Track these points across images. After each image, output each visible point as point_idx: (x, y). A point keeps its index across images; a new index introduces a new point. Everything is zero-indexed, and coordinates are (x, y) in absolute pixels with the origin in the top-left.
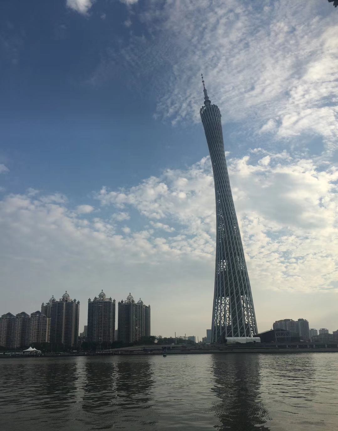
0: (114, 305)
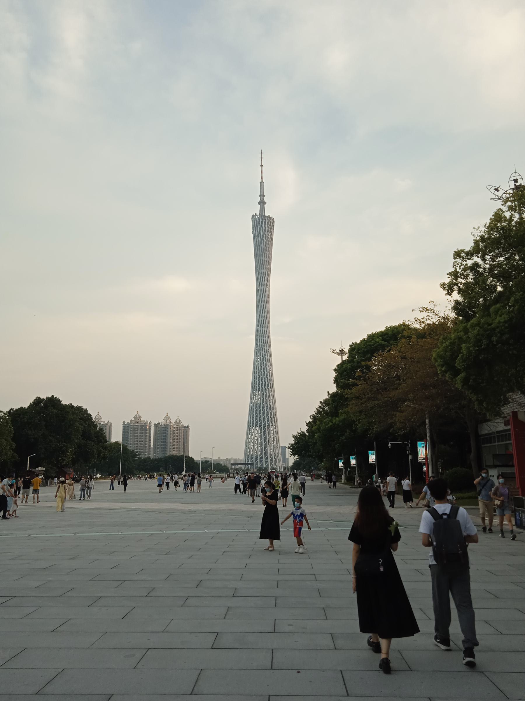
0: (150, 428)
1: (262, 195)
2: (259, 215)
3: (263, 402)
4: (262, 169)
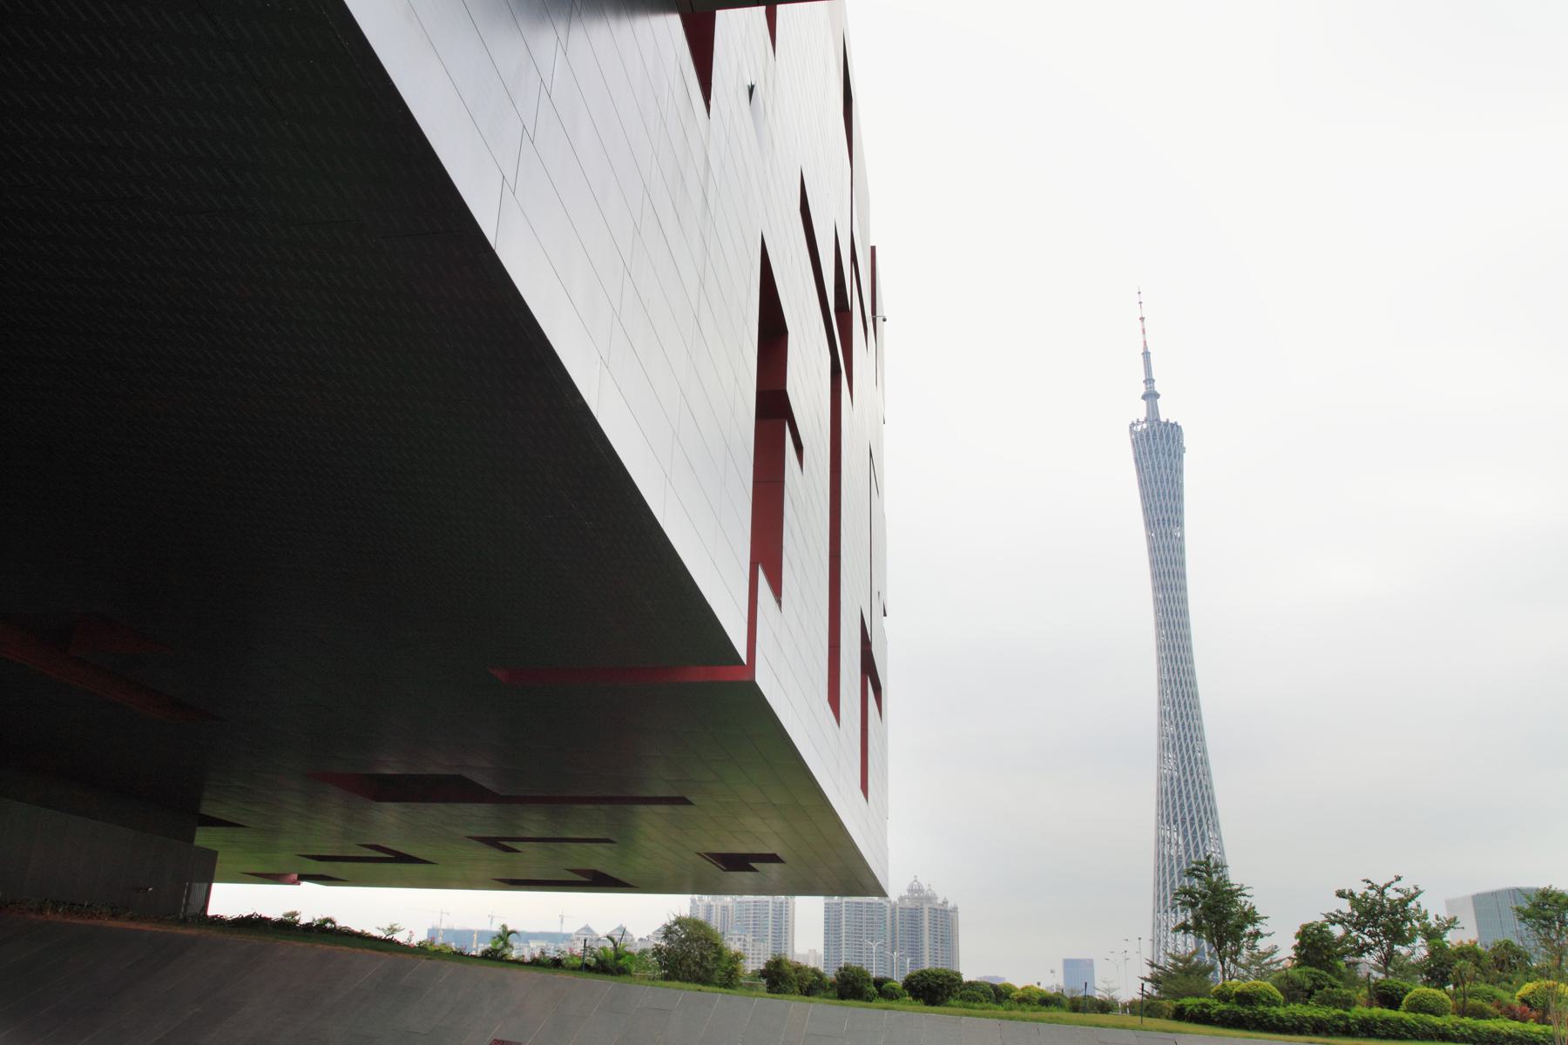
1: (1149, 380)
2: (1146, 420)
4: (1143, 325)
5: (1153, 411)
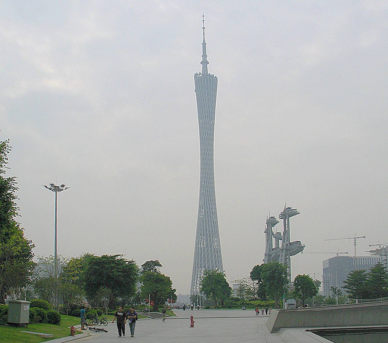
1: (205, 56)
3: (207, 246)
4: (204, 31)
5: (205, 69)
